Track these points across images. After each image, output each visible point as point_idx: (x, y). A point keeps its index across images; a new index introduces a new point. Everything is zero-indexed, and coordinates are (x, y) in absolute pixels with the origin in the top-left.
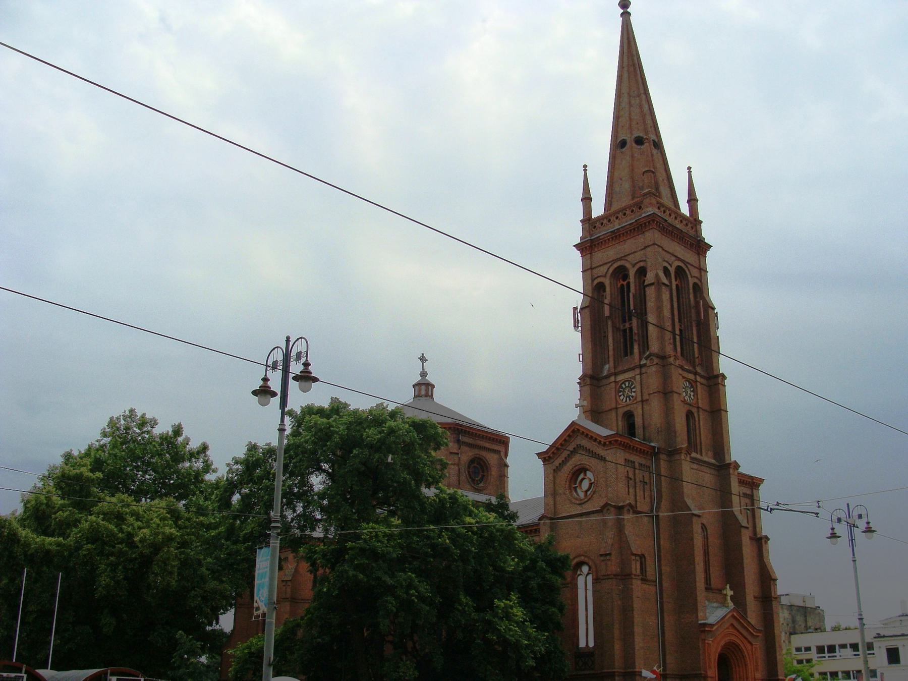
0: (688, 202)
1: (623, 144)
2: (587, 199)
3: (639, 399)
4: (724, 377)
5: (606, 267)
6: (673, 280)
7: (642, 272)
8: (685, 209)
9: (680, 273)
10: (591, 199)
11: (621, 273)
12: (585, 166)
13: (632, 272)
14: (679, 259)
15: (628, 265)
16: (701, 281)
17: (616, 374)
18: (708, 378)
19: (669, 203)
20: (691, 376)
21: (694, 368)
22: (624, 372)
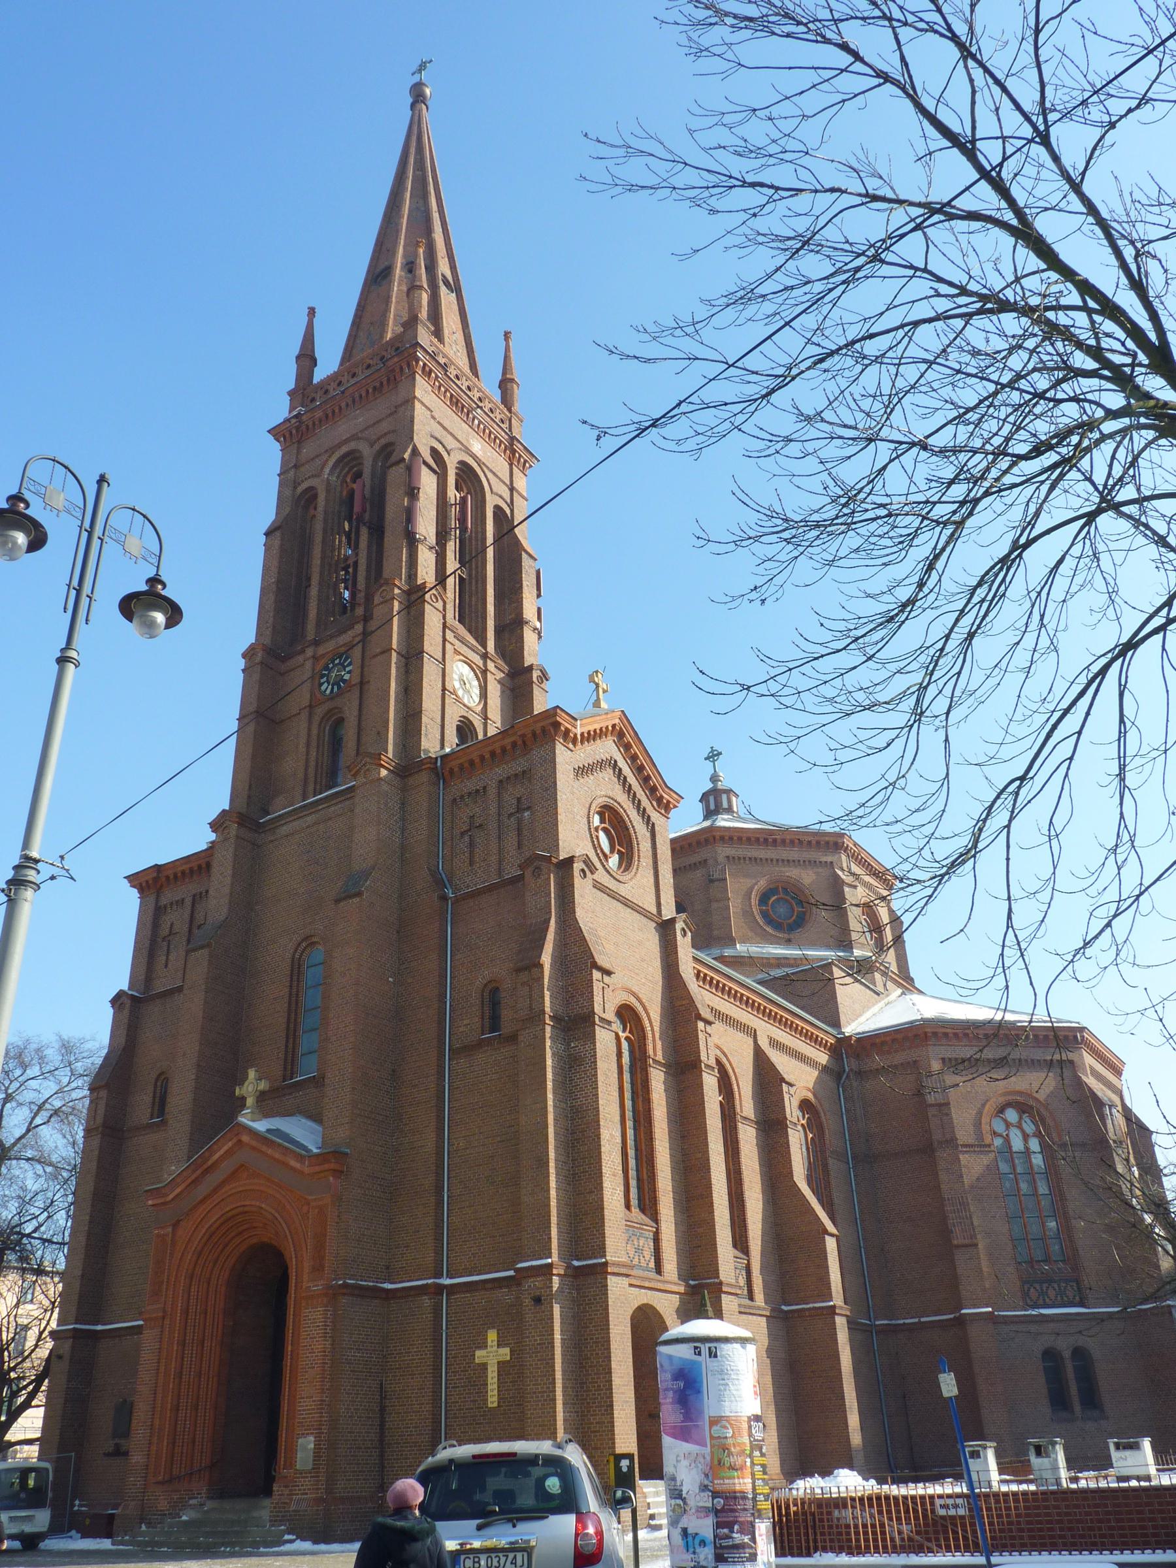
2: (307, 358)
3: (356, 680)
5: (324, 458)
10: (314, 362)
12: (312, 312)
13: (367, 452)
16: (512, 511)
17: (316, 643)
21: (484, 646)
22: (332, 637)
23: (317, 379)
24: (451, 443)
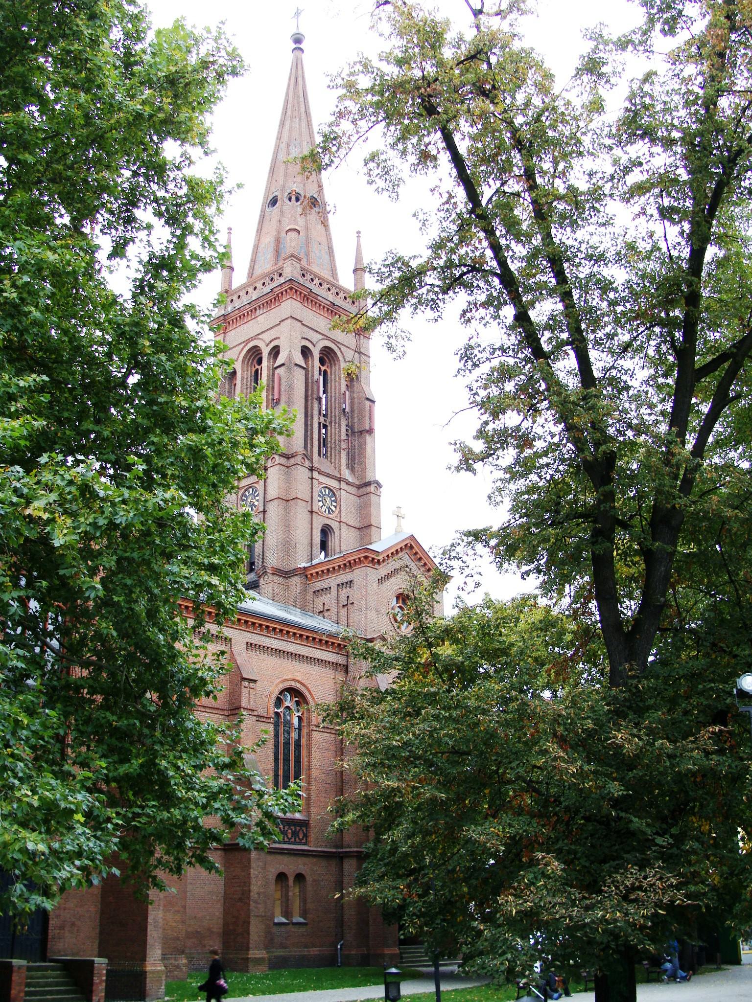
0: (355, 271)
1: (274, 202)
3: (261, 509)
4: (379, 485)
6: (317, 364)
7: (275, 352)
8: (347, 281)
9: (328, 356)
11: (255, 355)
14: (328, 338)
15: (261, 345)
18: (359, 487)
19: (326, 274)
20: (334, 484)
23: (235, 286)
24: (315, 337)
